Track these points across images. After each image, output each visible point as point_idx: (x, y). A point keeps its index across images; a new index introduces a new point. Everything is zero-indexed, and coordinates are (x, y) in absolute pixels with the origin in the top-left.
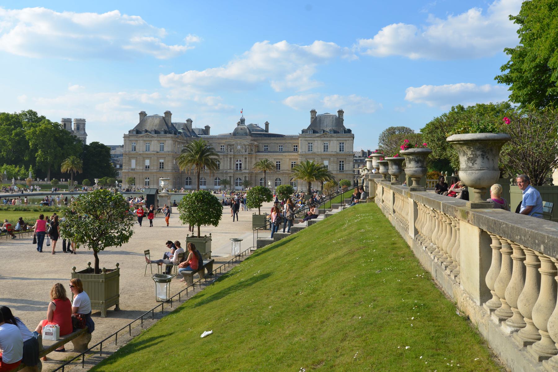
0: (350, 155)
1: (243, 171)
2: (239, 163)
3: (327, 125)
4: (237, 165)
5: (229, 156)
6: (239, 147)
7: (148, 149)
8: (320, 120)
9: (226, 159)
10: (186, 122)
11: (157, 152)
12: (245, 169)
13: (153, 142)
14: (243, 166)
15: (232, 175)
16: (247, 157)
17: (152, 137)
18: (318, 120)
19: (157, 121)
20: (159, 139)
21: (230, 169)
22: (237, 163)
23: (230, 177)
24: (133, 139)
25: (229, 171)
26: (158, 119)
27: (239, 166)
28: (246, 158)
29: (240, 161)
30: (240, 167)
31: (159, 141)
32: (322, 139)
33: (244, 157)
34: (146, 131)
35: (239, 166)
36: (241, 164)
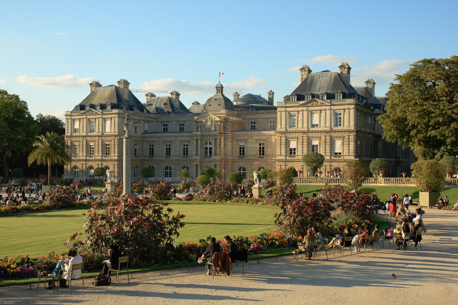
2: (209, 146)
3: (320, 88)
4: (206, 148)
8: (312, 80)
10: (170, 96)
12: (216, 154)
14: (213, 150)
15: (199, 163)
17: (97, 114)
18: (309, 81)
20: (104, 116)
21: (197, 154)
22: (206, 146)
23: (197, 165)
25: (194, 158)
28: (216, 139)
29: (210, 144)
30: (211, 152)
32: (309, 108)
34: (93, 106)
36: (211, 149)
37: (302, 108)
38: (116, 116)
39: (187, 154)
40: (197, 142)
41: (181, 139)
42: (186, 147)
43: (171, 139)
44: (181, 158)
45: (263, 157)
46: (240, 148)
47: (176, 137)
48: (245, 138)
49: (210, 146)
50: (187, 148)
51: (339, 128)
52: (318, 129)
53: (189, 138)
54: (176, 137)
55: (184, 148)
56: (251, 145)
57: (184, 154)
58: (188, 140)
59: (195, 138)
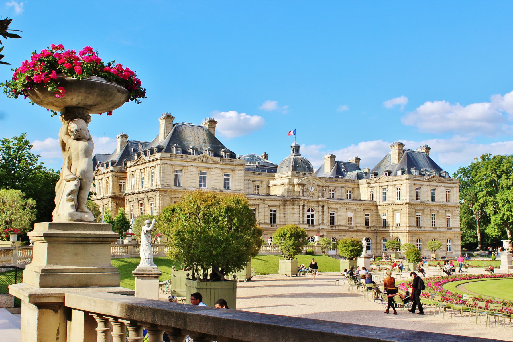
0: (457, 207)
1: (317, 227)
4: (308, 216)
5: (301, 203)
6: (311, 189)
7: (202, 182)
9: (289, 206)
11: (221, 191)
13: (213, 172)
16: (325, 204)
17: (213, 162)
18: (410, 156)
19: (203, 136)
20: (224, 167)
24: (177, 163)
26: (201, 130)
27: (310, 218)
28: (323, 207)
29: (312, 211)
31: (222, 169)
33: (321, 204)
35: (310, 218)
36: (313, 216)
37: (425, 183)
38: (241, 168)
39: (274, 222)
40: (303, 209)
41: (270, 203)
42: (273, 213)
43: (257, 202)
44: (270, 226)
45: (353, 227)
46: (331, 217)
47: (264, 200)
48: (337, 206)
49: (313, 213)
50: (275, 215)
51: (448, 203)
52: (436, 203)
53: (278, 202)
54: (264, 200)
55: (271, 215)
56: (342, 215)
57: (271, 222)
58: (278, 204)
59: (301, 203)
